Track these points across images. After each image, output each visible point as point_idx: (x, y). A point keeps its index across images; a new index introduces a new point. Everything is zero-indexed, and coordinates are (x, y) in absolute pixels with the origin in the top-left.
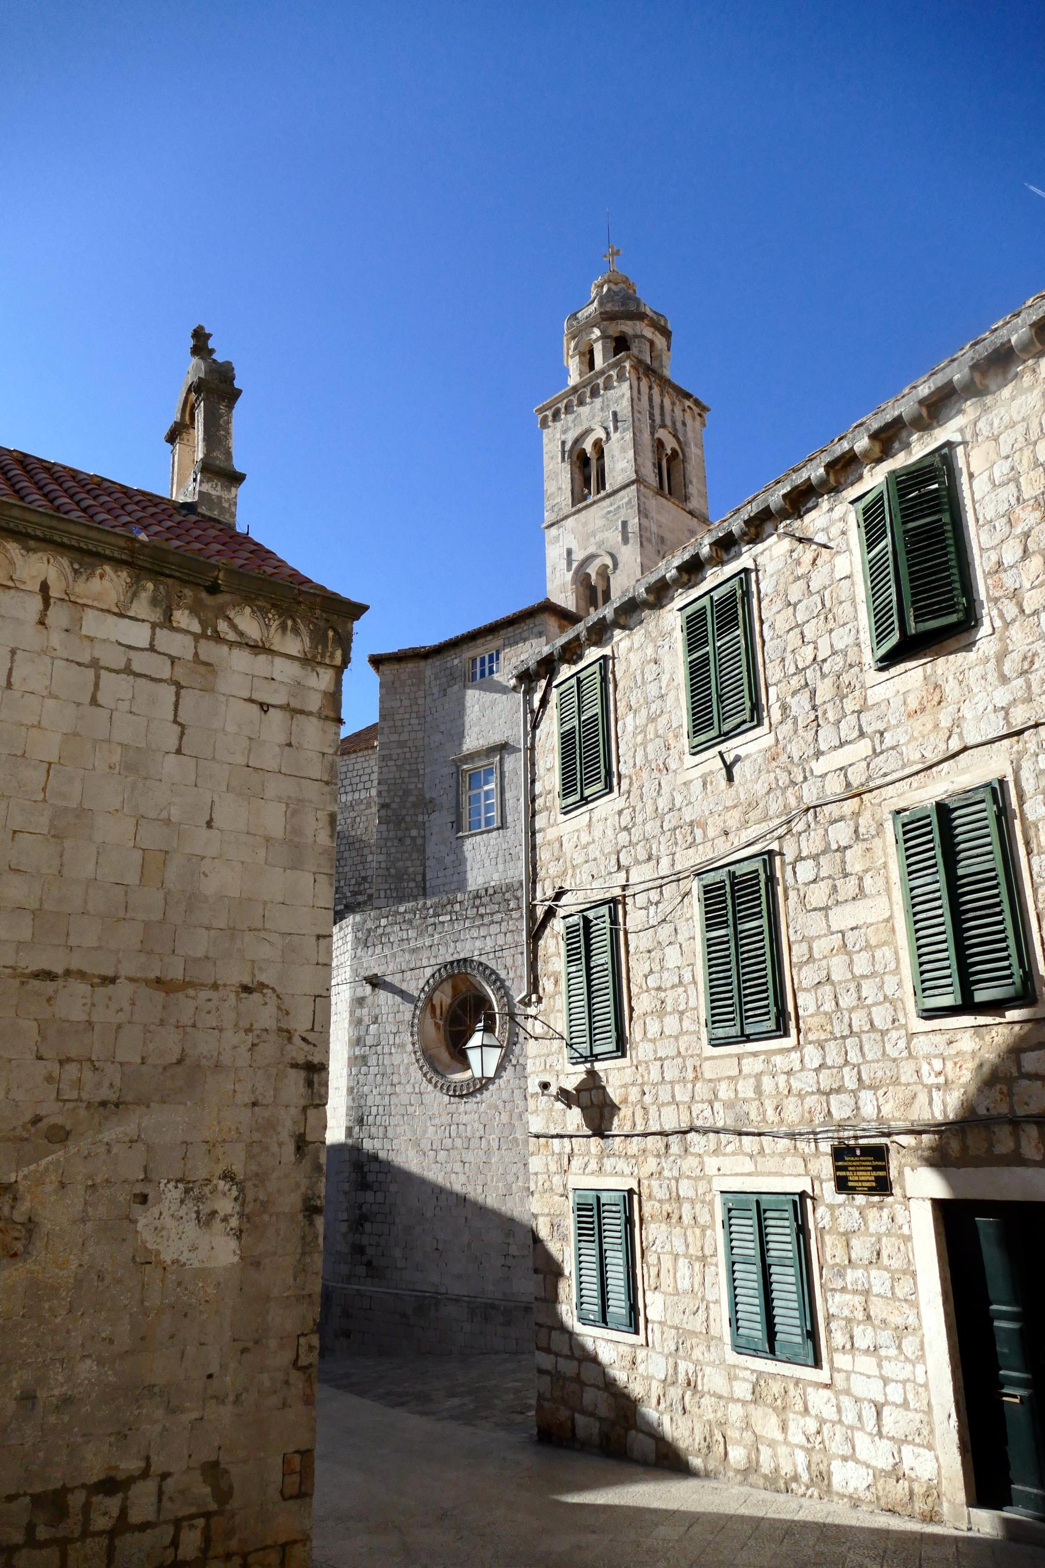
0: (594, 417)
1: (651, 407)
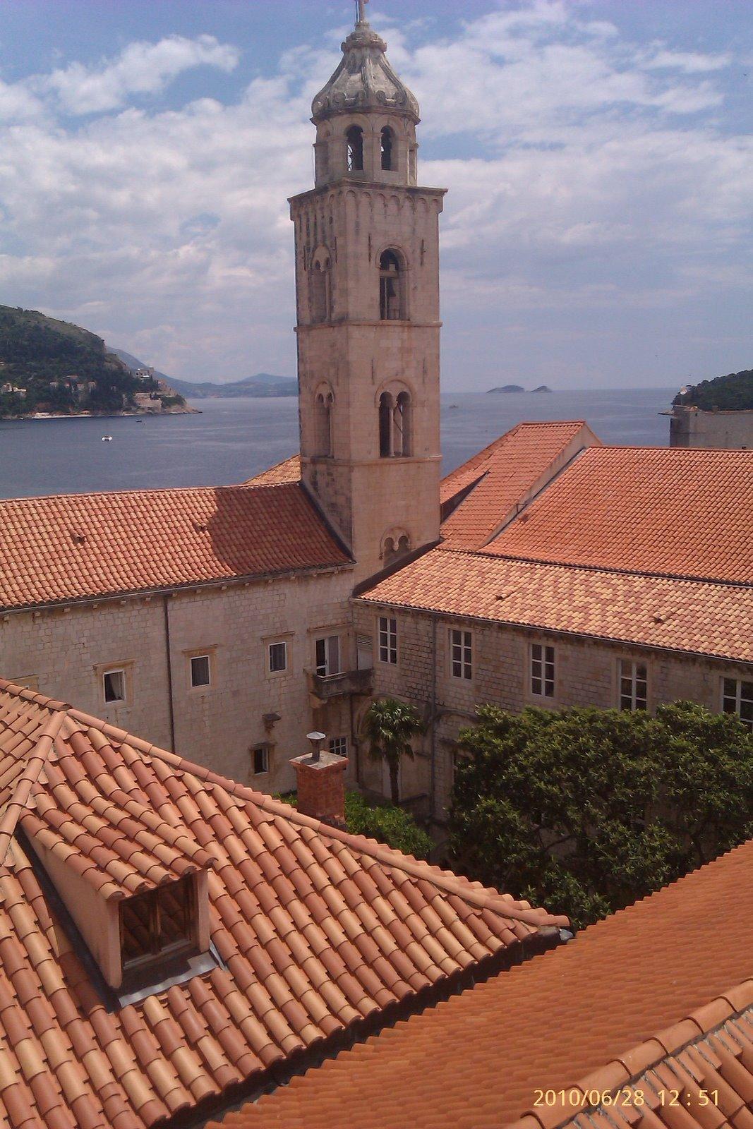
1: (308, 235)
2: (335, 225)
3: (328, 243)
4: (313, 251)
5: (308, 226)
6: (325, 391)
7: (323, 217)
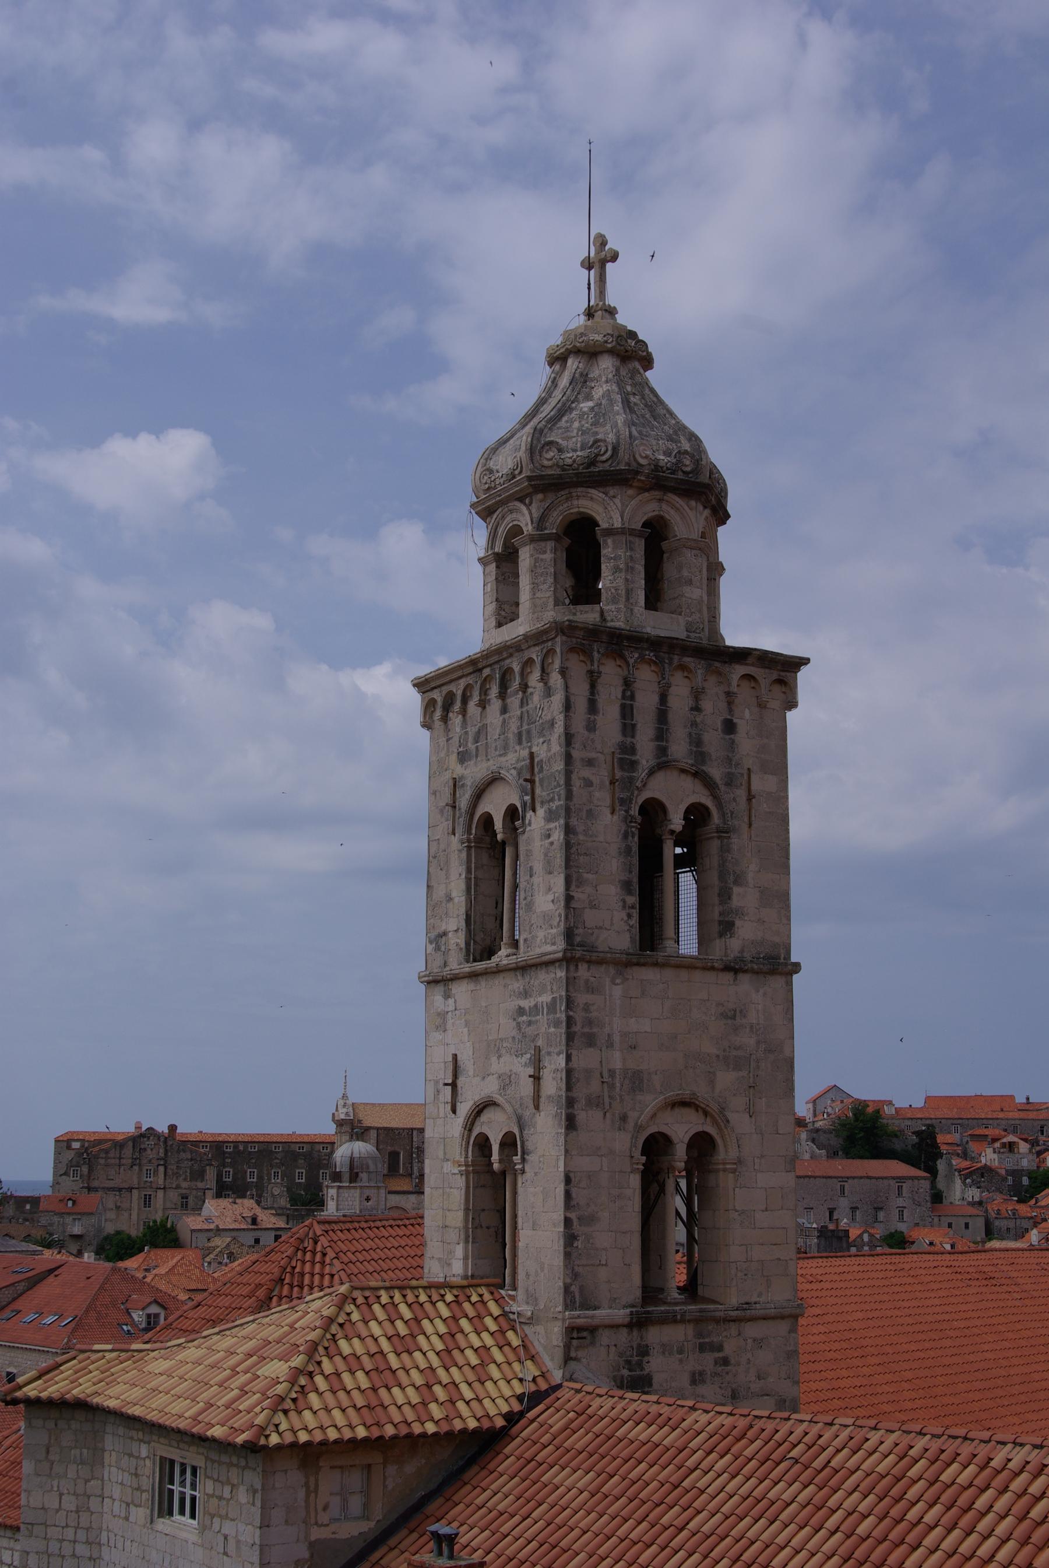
0: (506, 747)
1: (628, 728)
2: (746, 743)
3: (716, 772)
4: (651, 773)
5: (627, 712)
6: (681, 1129)
7: (696, 709)
